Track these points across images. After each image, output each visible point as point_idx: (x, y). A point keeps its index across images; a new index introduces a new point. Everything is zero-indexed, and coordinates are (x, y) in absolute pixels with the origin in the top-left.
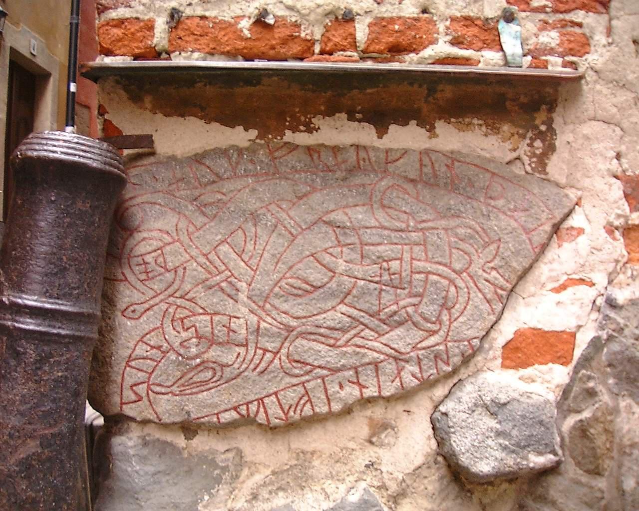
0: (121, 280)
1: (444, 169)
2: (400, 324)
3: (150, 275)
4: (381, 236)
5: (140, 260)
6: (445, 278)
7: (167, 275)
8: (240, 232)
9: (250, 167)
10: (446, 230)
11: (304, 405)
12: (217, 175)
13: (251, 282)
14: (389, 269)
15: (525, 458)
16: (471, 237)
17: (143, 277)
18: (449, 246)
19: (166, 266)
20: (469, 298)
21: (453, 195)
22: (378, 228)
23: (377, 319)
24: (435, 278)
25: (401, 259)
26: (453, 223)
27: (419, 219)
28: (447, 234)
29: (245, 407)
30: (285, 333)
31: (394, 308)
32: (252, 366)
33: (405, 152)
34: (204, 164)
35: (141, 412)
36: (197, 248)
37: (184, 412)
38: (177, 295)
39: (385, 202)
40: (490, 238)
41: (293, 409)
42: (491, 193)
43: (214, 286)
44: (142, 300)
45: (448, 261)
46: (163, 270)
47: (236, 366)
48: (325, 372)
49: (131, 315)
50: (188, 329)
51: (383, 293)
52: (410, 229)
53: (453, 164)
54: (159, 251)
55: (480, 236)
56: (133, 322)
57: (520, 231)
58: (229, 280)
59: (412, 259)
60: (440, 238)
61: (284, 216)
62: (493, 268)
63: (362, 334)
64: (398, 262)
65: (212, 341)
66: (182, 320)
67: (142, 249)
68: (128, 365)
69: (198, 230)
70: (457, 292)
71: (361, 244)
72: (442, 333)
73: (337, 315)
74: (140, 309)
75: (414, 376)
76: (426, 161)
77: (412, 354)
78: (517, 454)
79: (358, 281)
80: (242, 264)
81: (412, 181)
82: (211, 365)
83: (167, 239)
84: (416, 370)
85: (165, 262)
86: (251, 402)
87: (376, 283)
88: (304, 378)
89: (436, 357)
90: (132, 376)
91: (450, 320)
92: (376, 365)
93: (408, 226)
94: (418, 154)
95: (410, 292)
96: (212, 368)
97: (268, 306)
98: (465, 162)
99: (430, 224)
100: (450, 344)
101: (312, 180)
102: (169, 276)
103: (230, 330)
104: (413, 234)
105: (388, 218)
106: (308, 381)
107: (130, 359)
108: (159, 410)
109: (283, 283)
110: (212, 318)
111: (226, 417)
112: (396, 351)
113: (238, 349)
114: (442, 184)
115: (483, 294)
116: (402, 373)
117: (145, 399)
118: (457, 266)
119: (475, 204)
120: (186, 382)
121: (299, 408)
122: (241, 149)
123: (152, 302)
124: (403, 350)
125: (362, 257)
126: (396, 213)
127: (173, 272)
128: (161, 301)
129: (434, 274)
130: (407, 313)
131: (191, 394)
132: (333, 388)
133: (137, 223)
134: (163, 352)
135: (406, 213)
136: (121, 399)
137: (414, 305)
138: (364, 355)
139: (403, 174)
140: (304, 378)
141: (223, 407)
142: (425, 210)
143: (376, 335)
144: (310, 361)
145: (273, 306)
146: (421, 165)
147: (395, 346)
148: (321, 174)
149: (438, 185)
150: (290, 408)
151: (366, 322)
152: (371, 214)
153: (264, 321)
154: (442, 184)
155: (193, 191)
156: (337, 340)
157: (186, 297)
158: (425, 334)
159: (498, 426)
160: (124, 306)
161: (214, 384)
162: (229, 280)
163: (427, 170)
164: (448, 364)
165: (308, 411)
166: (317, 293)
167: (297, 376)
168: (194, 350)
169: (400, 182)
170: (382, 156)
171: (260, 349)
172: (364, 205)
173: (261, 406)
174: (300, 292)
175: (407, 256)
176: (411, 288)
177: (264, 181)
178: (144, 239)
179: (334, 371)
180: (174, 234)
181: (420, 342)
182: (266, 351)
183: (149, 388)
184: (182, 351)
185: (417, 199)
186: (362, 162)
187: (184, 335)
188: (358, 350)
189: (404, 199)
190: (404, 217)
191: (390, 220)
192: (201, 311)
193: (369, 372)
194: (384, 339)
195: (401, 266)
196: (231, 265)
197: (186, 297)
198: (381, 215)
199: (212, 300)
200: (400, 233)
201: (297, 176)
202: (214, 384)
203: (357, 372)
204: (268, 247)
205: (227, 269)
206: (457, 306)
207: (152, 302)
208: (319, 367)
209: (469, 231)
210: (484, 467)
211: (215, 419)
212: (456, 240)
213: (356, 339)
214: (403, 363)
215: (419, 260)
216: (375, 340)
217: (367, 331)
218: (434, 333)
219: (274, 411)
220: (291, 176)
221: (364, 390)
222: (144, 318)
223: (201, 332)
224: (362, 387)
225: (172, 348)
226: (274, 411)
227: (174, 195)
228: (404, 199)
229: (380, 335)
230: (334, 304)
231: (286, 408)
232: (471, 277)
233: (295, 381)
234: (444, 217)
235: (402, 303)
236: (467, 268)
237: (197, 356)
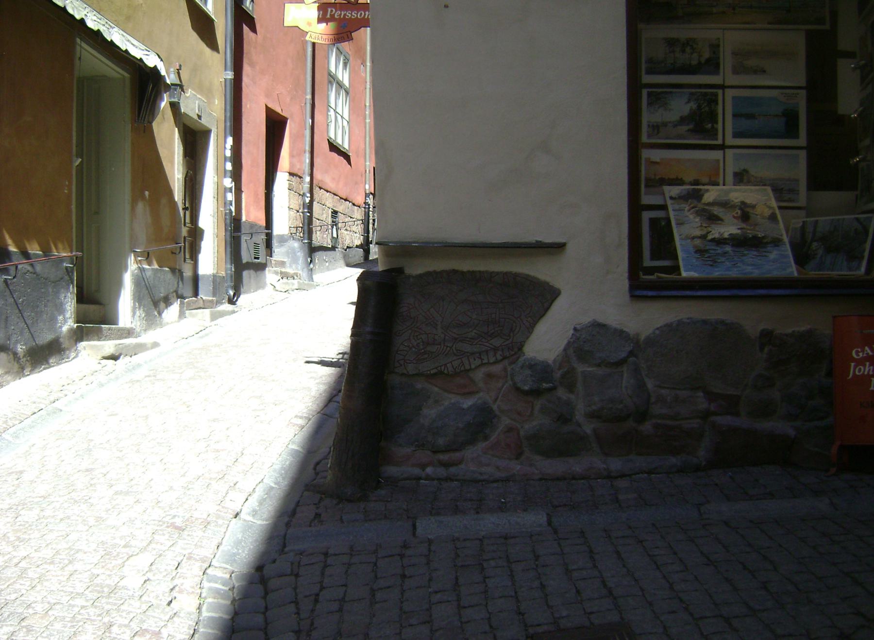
33: (498, 273)
92: (487, 352)
132: (472, 360)
165: (462, 369)
179: (472, 354)
210: (526, 388)
219: (450, 369)
226: (450, 369)
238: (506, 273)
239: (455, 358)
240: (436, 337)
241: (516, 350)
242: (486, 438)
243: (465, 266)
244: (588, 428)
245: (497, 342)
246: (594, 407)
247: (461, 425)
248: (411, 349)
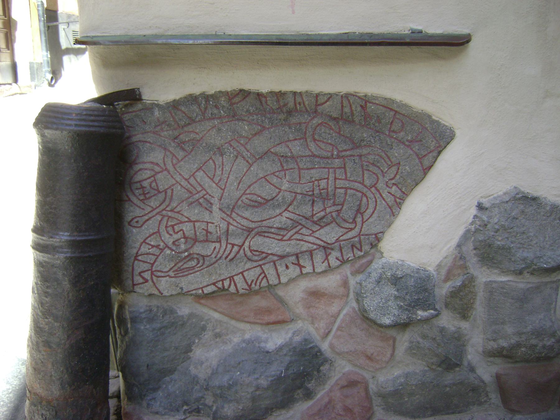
0: (126, 201)
1: (359, 109)
3: (147, 196)
5: (138, 185)
7: (160, 195)
8: (211, 161)
9: (216, 111)
11: (262, 279)
12: (190, 118)
13: (221, 198)
15: (416, 314)
17: (142, 197)
19: (158, 188)
23: (311, 221)
24: (352, 191)
27: (341, 149)
29: (221, 283)
30: (246, 234)
31: (323, 214)
32: (224, 256)
33: (330, 96)
34: (181, 110)
35: (147, 290)
36: (180, 174)
37: (178, 288)
38: (168, 209)
40: (392, 162)
41: (254, 282)
42: (393, 128)
43: (194, 202)
44: (143, 214)
46: (156, 192)
47: (213, 256)
48: (275, 258)
49: (135, 224)
50: (178, 232)
53: (366, 105)
54: (153, 178)
55: (385, 161)
56: (137, 229)
57: (414, 156)
58: (205, 197)
59: (335, 179)
61: (243, 149)
62: (394, 184)
65: (195, 240)
66: (173, 226)
67: (138, 178)
68: (136, 259)
69: (179, 161)
73: (283, 220)
74: (141, 220)
75: (337, 259)
76: (345, 103)
77: (336, 244)
78: (409, 311)
80: (214, 185)
81: (335, 119)
82: (195, 256)
83: (157, 169)
84: (338, 255)
85: (157, 185)
86: (225, 279)
87: (310, 196)
88: (261, 263)
89: (353, 246)
90: (139, 267)
92: (311, 253)
93: (332, 155)
94: (340, 97)
95: (334, 202)
96: (196, 258)
97: (234, 215)
98: (375, 103)
99: (348, 153)
100: (362, 237)
101: (262, 121)
102: (161, 196)
103: (207, 231)
106: (264, 264)
107: (137, 255)
108: (161, 288)
109: (244, 198)
110: (194, 224)
111: (207, 290)
112: (325, 242)
113: (214, 245)
116: (329, 257)
117: (150, 282)
119: (382, 136)
120: (178, 268)
121: (258, 282)
122: (208, 96)
123: (150, 215)
124: (329, 242)
127: (164, 193)
128: (156, 214)
129: (351, 189)
131: (183, 276)
132: (281, 269)
133: (134, 158)
134: (160, 249)
136: (133, 282)
137: (337, 211)
140: (261, 263)
141: (205, 284)
143: (311, 232)
144: (266, 251)
145: (237, 214)
146: (342, 106)
147: (324, 239)
148: (268, 116)
150: (252, 282)
151: (303, 223)
153: (232, 224)
155: (174, 131)
156: (284, 236)
157: (175, 210)
158: (345, 231)
159: (396, 293)
160: (130, 218)
161: (199, 269)
162: (205, 197)
163: (347, 110)
164: (361, 250)
166: (269, 204)
167: (256, 261)
168: (183, 247)
170: (313, 100)
171: (230, 244)
173: (232, 282)
174: (256, 204)
177: (226, 122)
178: (140, 170)
179: (282, 257)
180: (162, 165)
181: (342, 235)
182: (233, 245)
183: (152, 274)
184: (174, 248)
185: (339, 133)
186: (298, 106)
187: (176, 237)
188: (298, 242)
189: (329, 134)
192: (186, 220)
193: (306, 257)
194: (317, 234)
196: (206, 186)
197: (175, 210)
199: (194, 213)
200: (327, 160)
201: (251, 117)
202: (199, 269)
203: (298, 258)
204: (232, 173)
205: (204, 189)
206: (368, 211)
207: (150, 215)
208: (272, 254)
210: (387, 321)
211: (200, 291)
213: (296, 235)
214: (330, 251)
216: (310, 235)
217: (304, 229)
218: (351, 229)
220: (246, 118)
221: (303, 269)
222: (145, 226)
223: (187, 235)
224: (301, 267)
225: (167, 246)
227: (159, 135)
229: (313, 232)
230: (281, 211)
231: (249, 283)
233: (255, 264)
235: (328, 210)
236: (376, 184)
237: (186, 251)
238: (347, 96)
239: (249, 265)
240: (211, 228)
241: (366, 248)
242: (309, 395)
243: (265, 80)
244: (486, 372)
245: (330, 234)
246: (504, 343)
247: (264, 382)
248: (162, 250)
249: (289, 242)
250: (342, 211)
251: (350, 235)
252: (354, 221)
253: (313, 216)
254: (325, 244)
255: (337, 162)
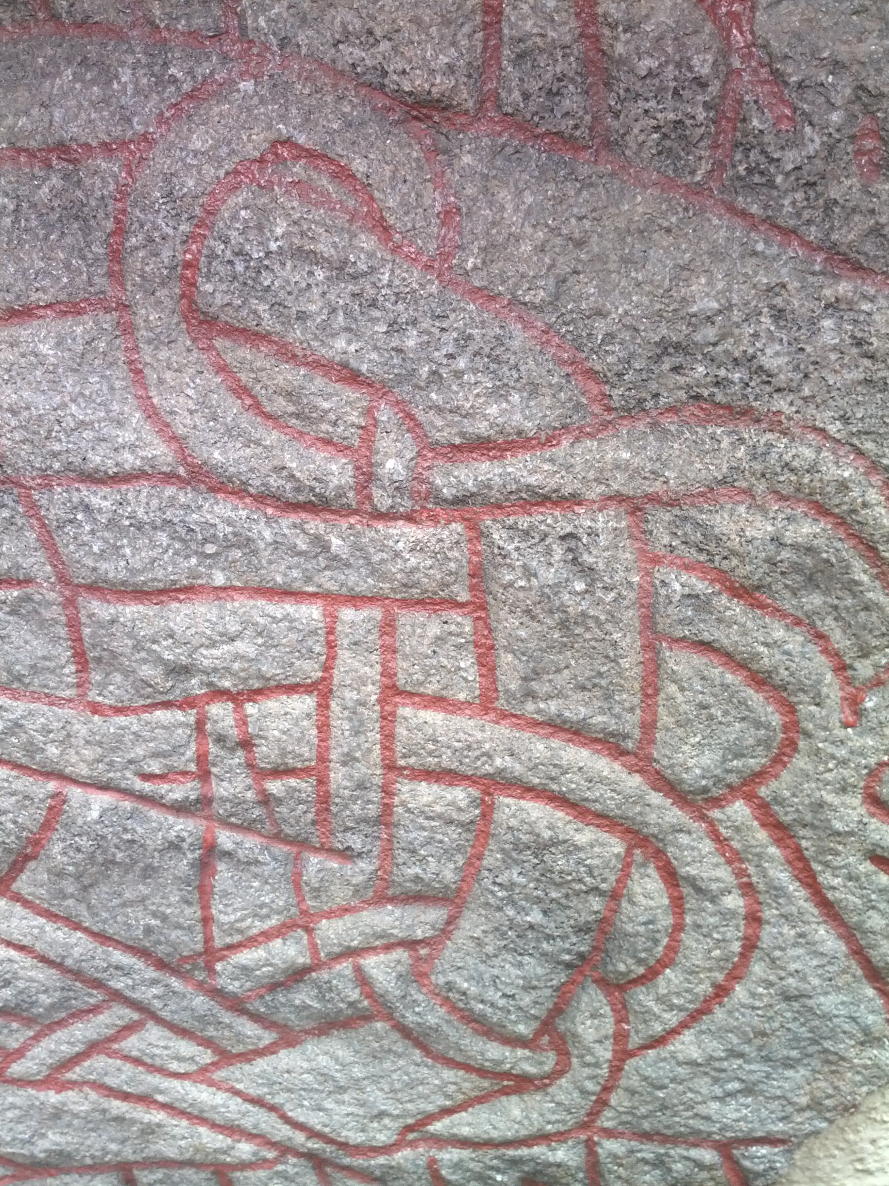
2: (329, 1025)
4: (188, 538)
6: (606, 821)
10: (635, 507)
14: (246, 744)
16: (817, 573)
18: (649, 621)
20: (750, 945)
21: (720, 228)
22: (170, 477)
24: (537, 812)
25: (322, 689)
26: (690, 456)
27: (443, 430)
28: (641, 534)
31: (289, 951)
39: (214, 292)
45: (631, 723)
51: (223, 875)
52: (382, 500)
59: (392, 691)
60: (588, 572)
63: (132, 1044)
64: (306, 703)
70: (678, 905)
71: (63, 579)
72: (564, 1090)
77: (402, 1156)
79: (75, 793)
81: (423, 111)
87: (180, 808)
91: (620, 1037)
93: (367, 477)
99: (524, 470)
100: (610, 1146)
104: (403, 534)
105: (232, 409)
114: (640, 136)
115: (850, 933)
118: (695, 759)
125: (81, 659)
126: (288, 375)
130: (362, 979)
135: (352, 377)
137: (410, 944)
138: (149, 1131)
139: (351, 53)
142: (493, 357)
143: (207, 1057)
149: (611, 145)
151: (148, 994)
152: (120, 377)
154: (640, 136)
158: (470, 1084)
169: (328, 121)
172: (70, 308)
175: (358, 673)
176: (387, 852)
181: (447, 1111)
185: (441, 264)
189: (340, 269)
190: (343, 405)
191: (247, 421)
194: (247, 1076)
195: (324, 728)
198: (187, 386)
200: (315, 525)
209: (807, 529)
212: (701, 586)
213: (99, 1063)
215: (438, 702)
216: (202, 1075)
217: (154, 1034)
218: (521, 1084)
228: (340, 269)
232: (781, 832)
234: (634, 410)
235: (333, 932)
236: (760, 776)
249: (52, 1097)
250: (449, 952)
251: (511, 1116)
252: (552, 1031)
253: (211, 955)
254: (314, 1145)
255: (414, 546)
